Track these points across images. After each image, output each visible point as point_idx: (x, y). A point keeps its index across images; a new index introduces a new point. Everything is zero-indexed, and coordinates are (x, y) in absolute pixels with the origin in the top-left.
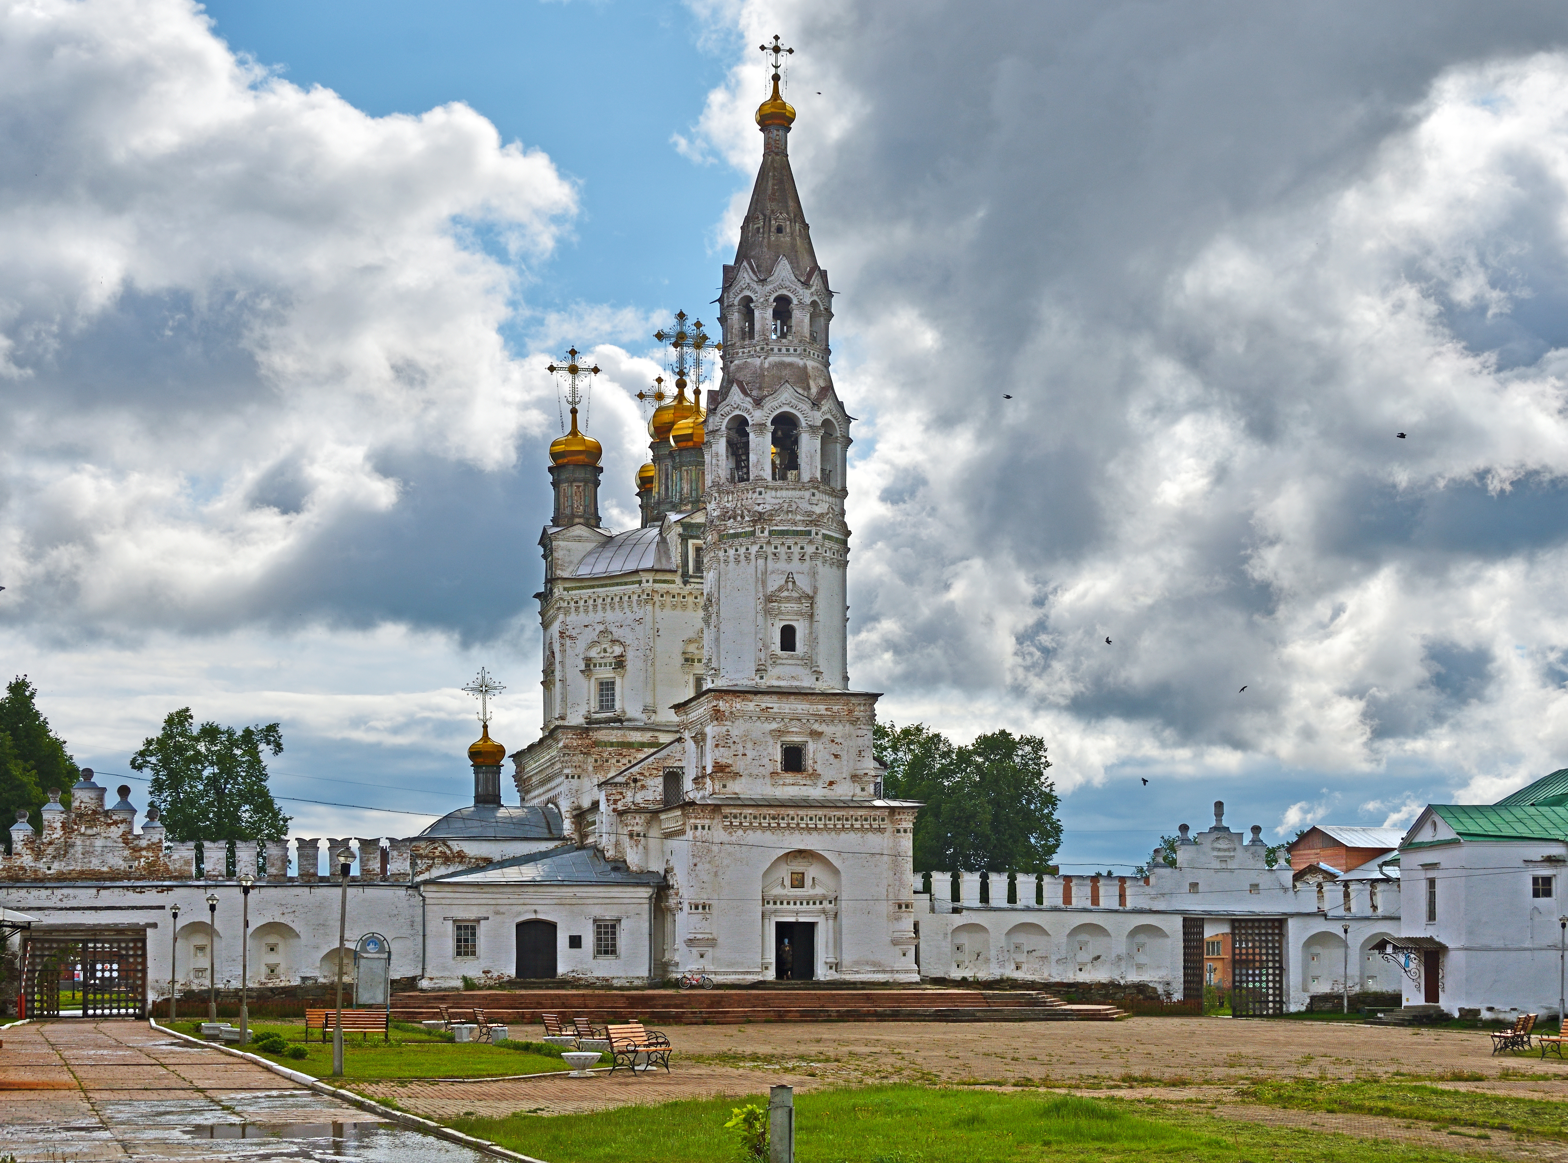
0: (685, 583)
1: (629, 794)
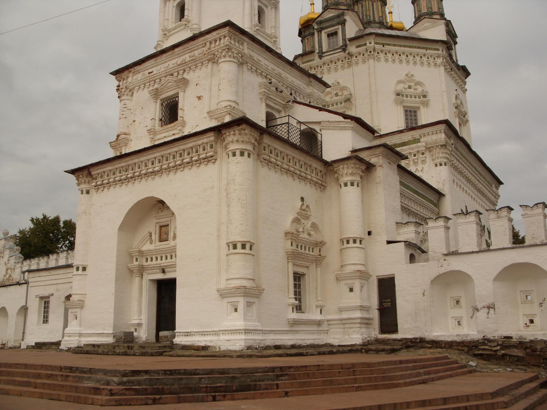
0: (320, 57)
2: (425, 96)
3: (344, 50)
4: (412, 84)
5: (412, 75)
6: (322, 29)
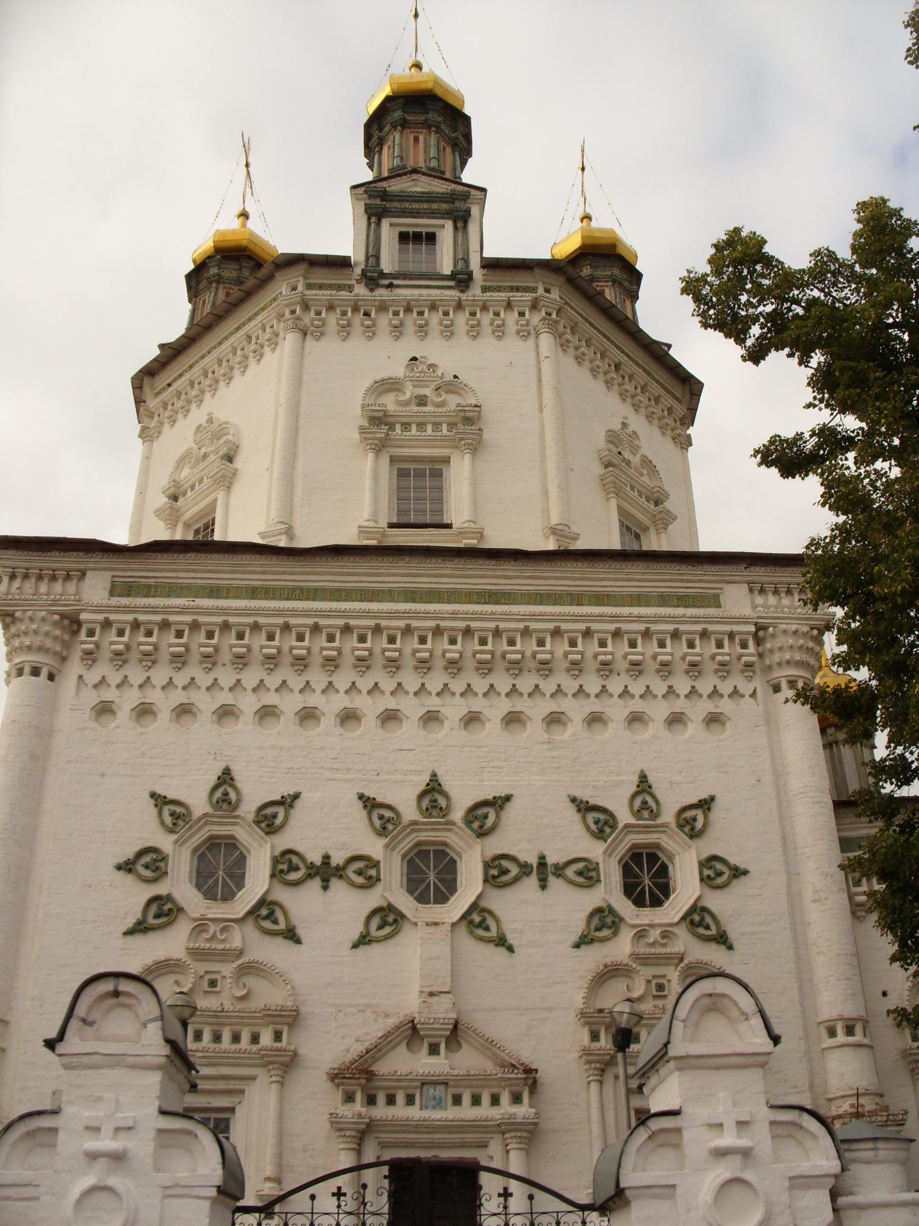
2: (468, 421)
4: (427, 391)
5: (432, 366)
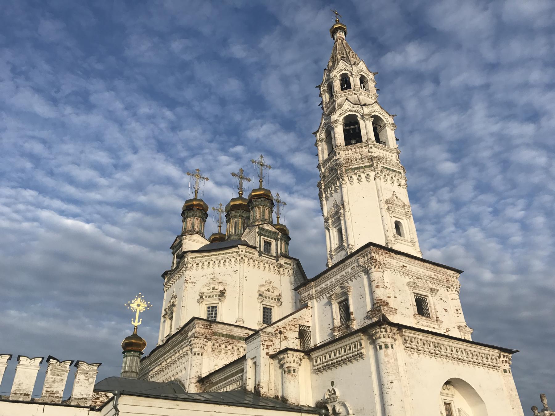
1: (276, 341)
3: (277, 260)
6: (263, 235)
